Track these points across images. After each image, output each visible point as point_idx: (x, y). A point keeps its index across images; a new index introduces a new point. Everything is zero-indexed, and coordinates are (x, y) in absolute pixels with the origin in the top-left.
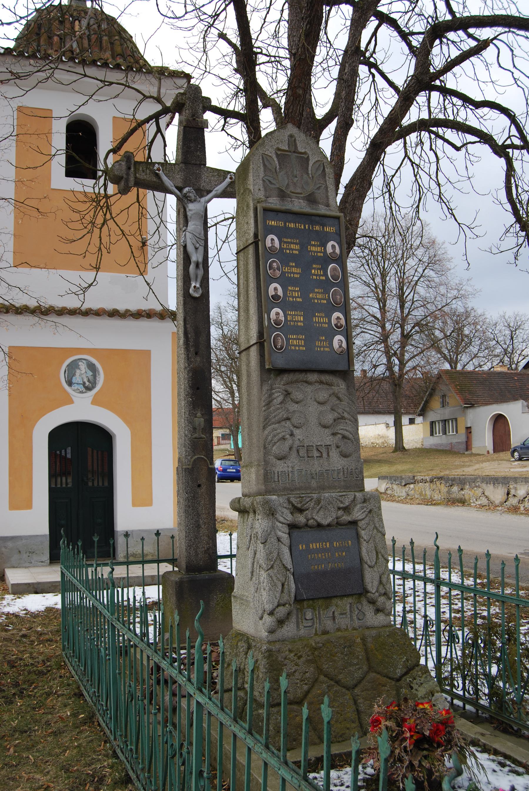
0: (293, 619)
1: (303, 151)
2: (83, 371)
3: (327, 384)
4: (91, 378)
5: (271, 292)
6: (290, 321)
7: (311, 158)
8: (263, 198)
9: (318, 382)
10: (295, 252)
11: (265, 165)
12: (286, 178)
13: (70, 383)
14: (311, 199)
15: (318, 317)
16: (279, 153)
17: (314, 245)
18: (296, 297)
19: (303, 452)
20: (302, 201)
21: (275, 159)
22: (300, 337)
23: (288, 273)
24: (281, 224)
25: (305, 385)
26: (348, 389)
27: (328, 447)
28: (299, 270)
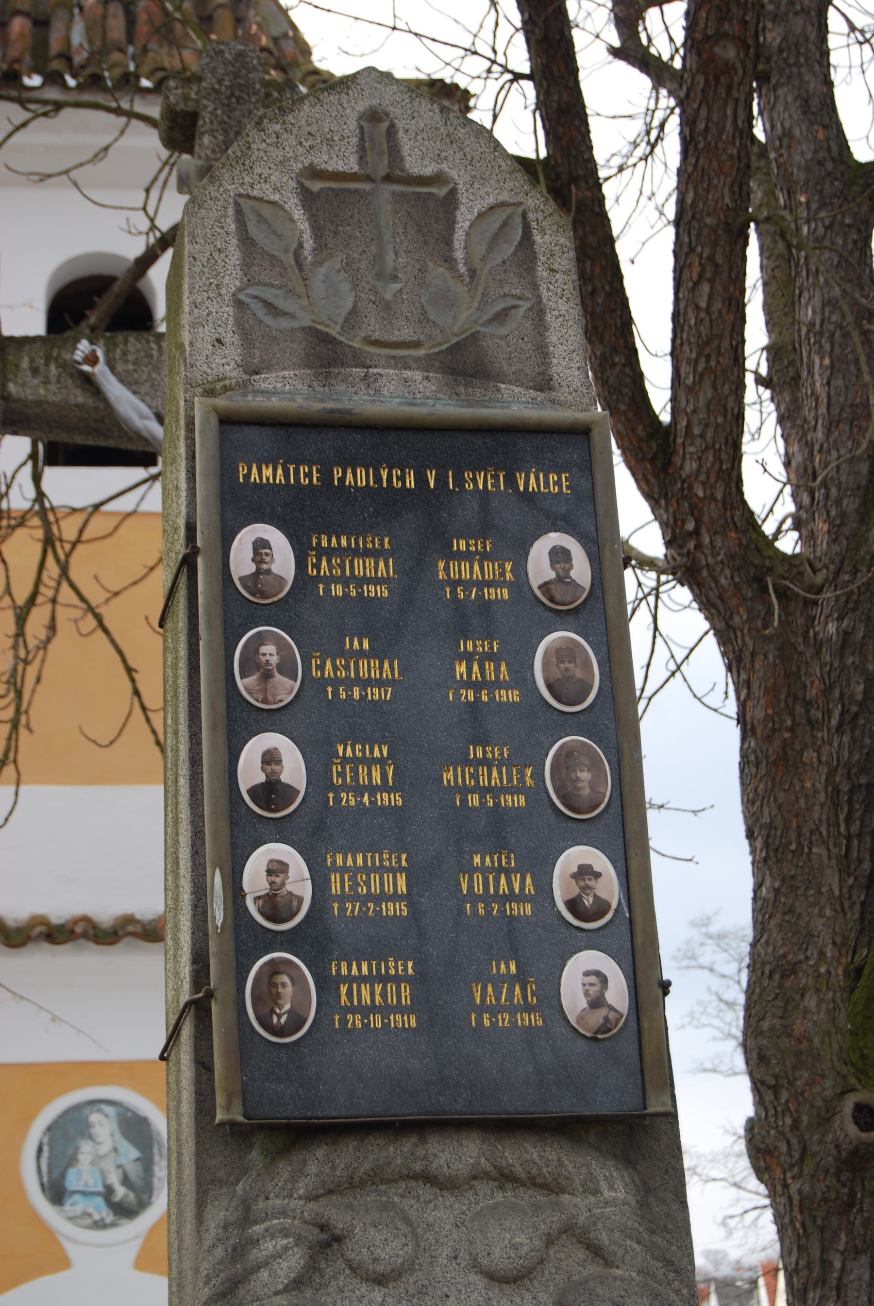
1: (429, 170)
2: (106, 1147)
3: (535, 1183)
4: (135, 1172)
5: (250, 772)
6: (342, 898)
7: (463, 196)
8: (232, 373)
9: (486, 1176)
10: (371, 591)
11: (246, 241)
12: (346, 287)
13: (57, 1193)
14: (463, 363)
15: (484, 871)
16: (316, 186)
17: (468, 556)
18: (373, 790)
20: (418, 375)
21: (298, 214)
22: (393, 967)
23: (336, 682)
24: (308, 475)
25: (425, 1192)
26: (643, 1205)
28: (389, 670)
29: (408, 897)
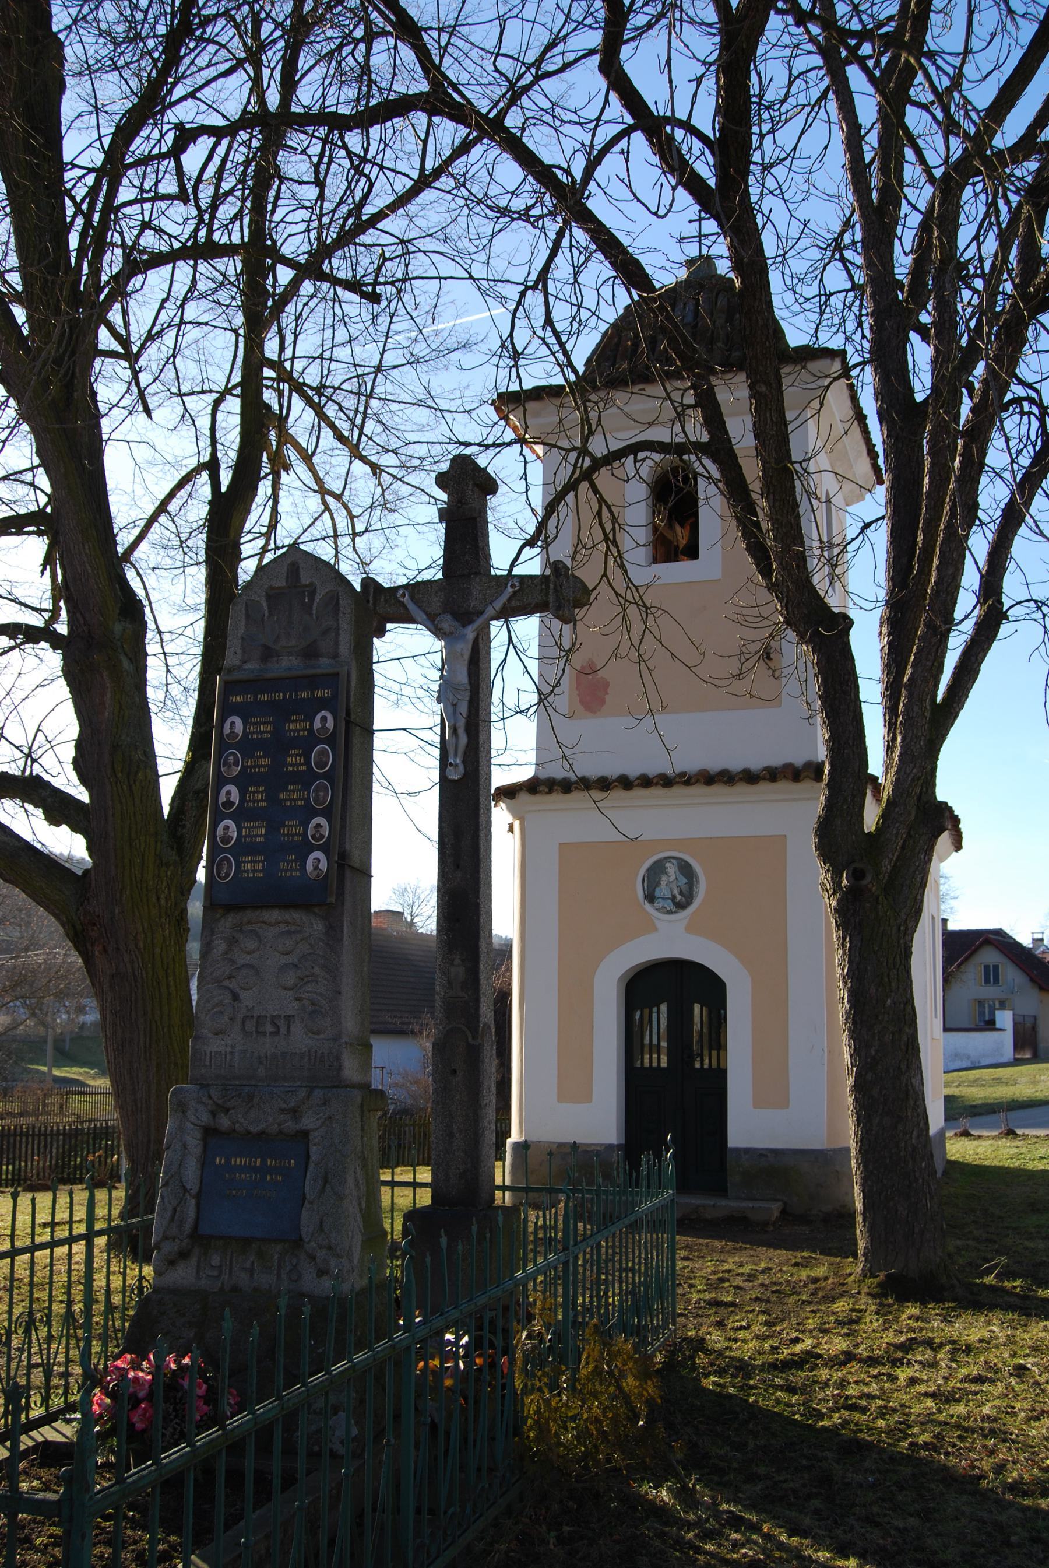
0: (193, 1261)
2: (672, 878)
4: (685, 889)
10: (265, 736)
11: (248, 616)
13: (650, 898)
17: (296, 721)
19: (250, 1025)
21: (265, 604)
22: (258, 858)
24: (250, 698)
27: (289, 1018)
28: (268, 761)
29: (265, 836)
